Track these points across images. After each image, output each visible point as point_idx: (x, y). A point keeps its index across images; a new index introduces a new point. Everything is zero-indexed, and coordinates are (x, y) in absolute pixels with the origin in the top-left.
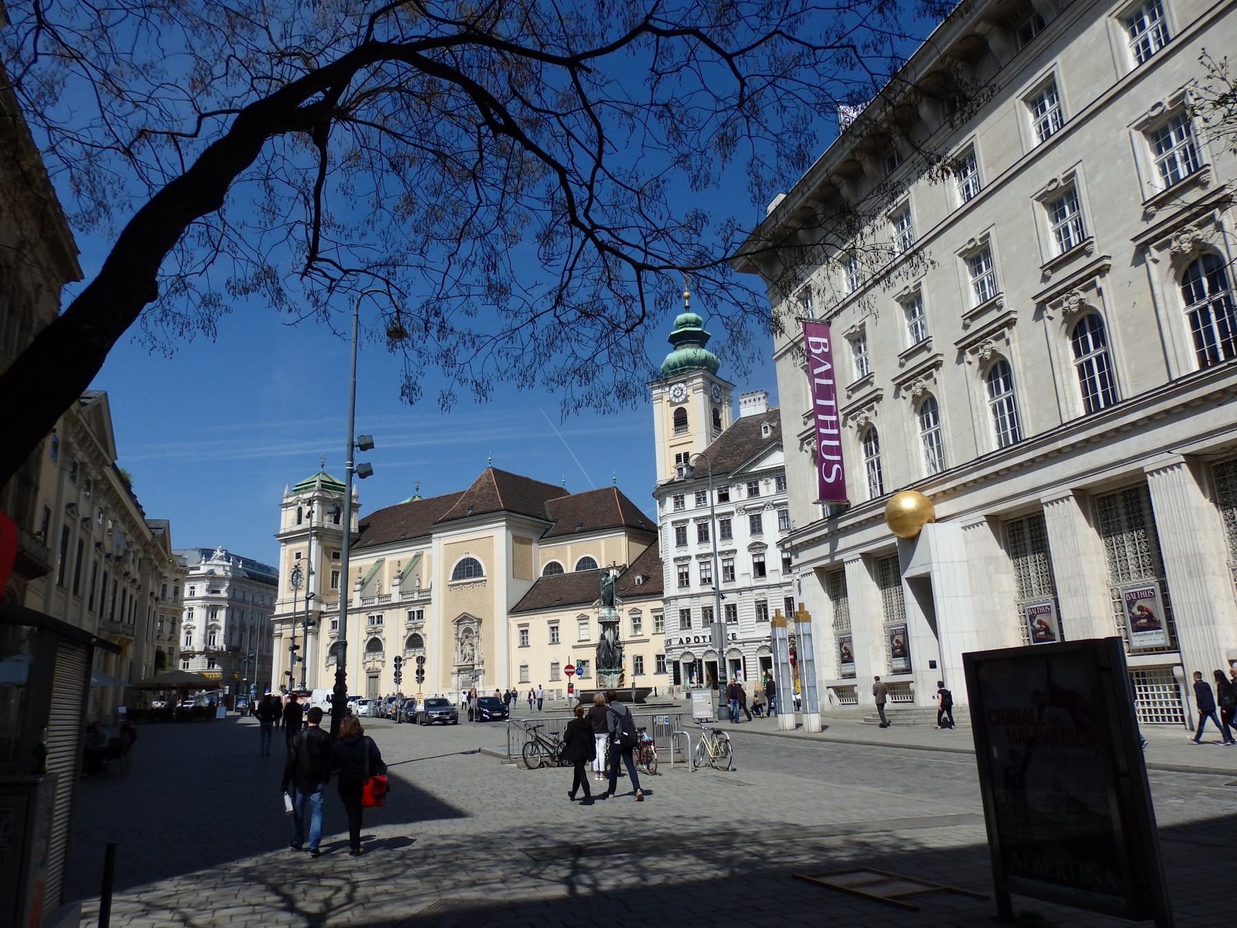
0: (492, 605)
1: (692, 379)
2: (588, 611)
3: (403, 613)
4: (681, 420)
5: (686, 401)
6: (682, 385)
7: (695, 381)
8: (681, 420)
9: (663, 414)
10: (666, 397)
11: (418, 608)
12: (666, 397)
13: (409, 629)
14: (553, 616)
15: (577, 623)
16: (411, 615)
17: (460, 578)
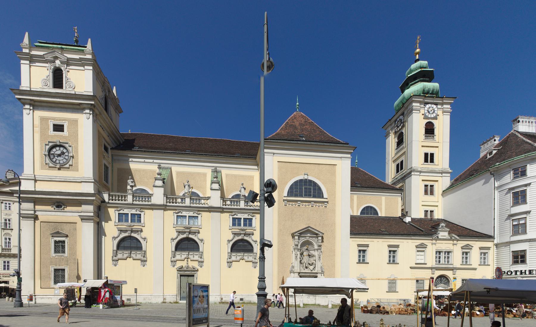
0: (333, 224)
1: (442, 104)
2: (427, 242)
3: (226, 219)
4: (430, 130)
5: (435, 118)
6: (435, 106)
7: (445, 106)
8: (430, 130)
9: (416, 123)
10: (422, 111)
11: (246, 216)
12: (422, 111)
13: (235, 234)
14: (394, 241)
15: (415, 249)
16: (236, 222)
17: (296, 196)
